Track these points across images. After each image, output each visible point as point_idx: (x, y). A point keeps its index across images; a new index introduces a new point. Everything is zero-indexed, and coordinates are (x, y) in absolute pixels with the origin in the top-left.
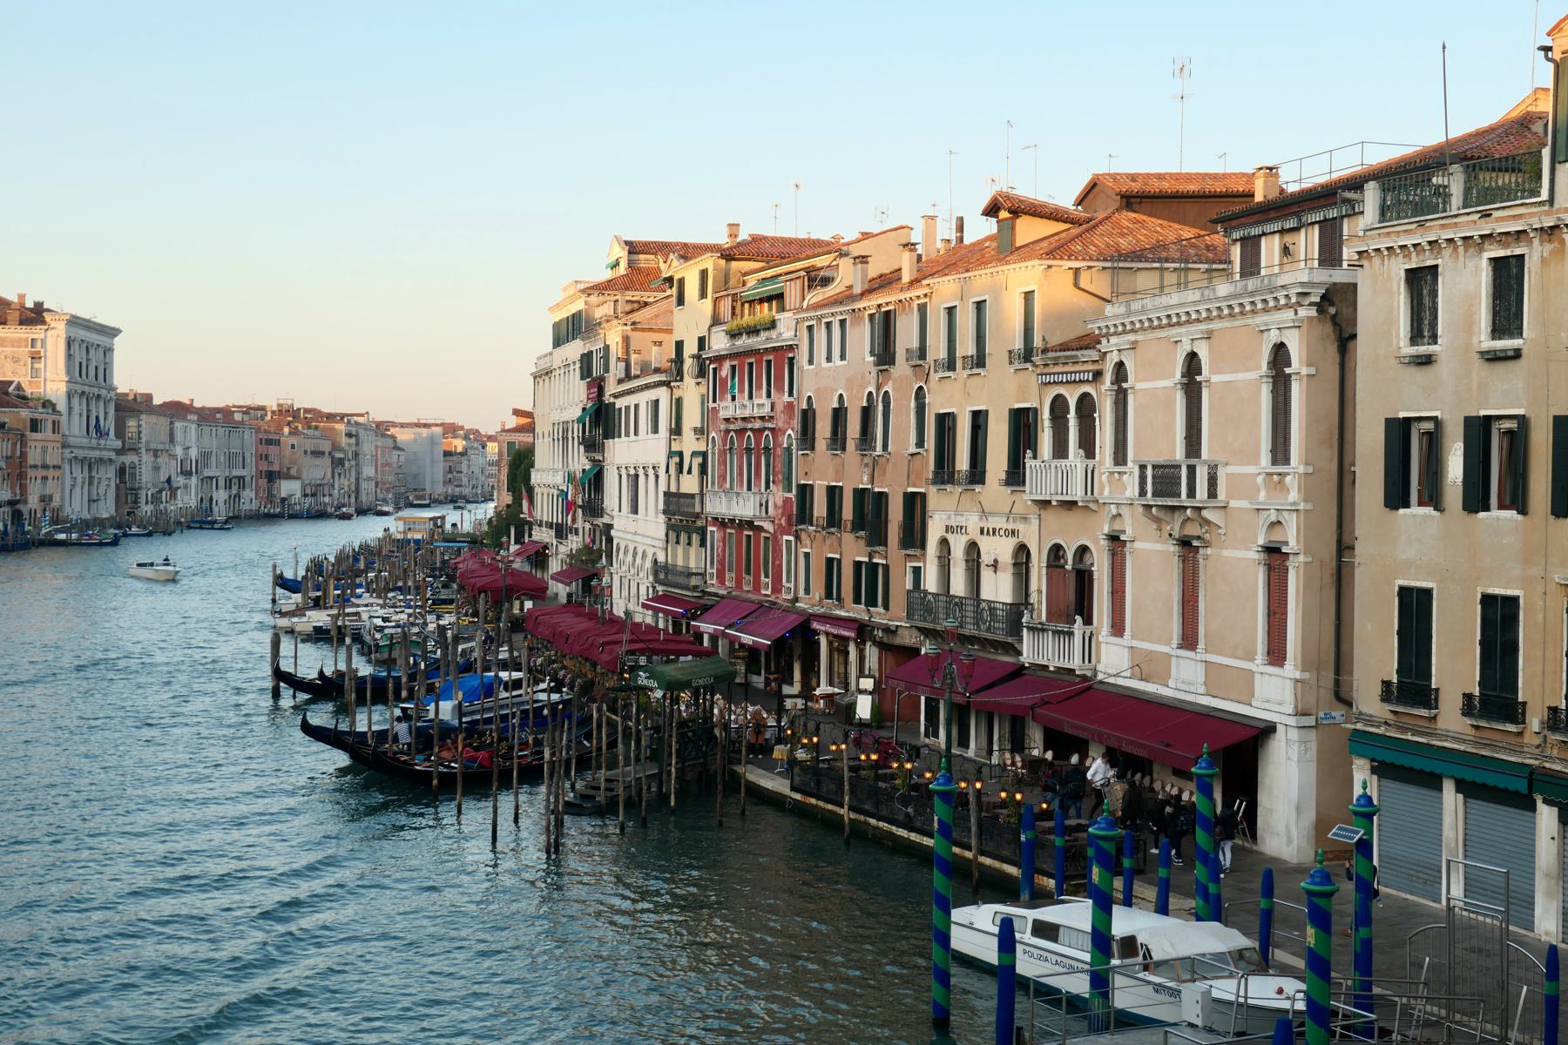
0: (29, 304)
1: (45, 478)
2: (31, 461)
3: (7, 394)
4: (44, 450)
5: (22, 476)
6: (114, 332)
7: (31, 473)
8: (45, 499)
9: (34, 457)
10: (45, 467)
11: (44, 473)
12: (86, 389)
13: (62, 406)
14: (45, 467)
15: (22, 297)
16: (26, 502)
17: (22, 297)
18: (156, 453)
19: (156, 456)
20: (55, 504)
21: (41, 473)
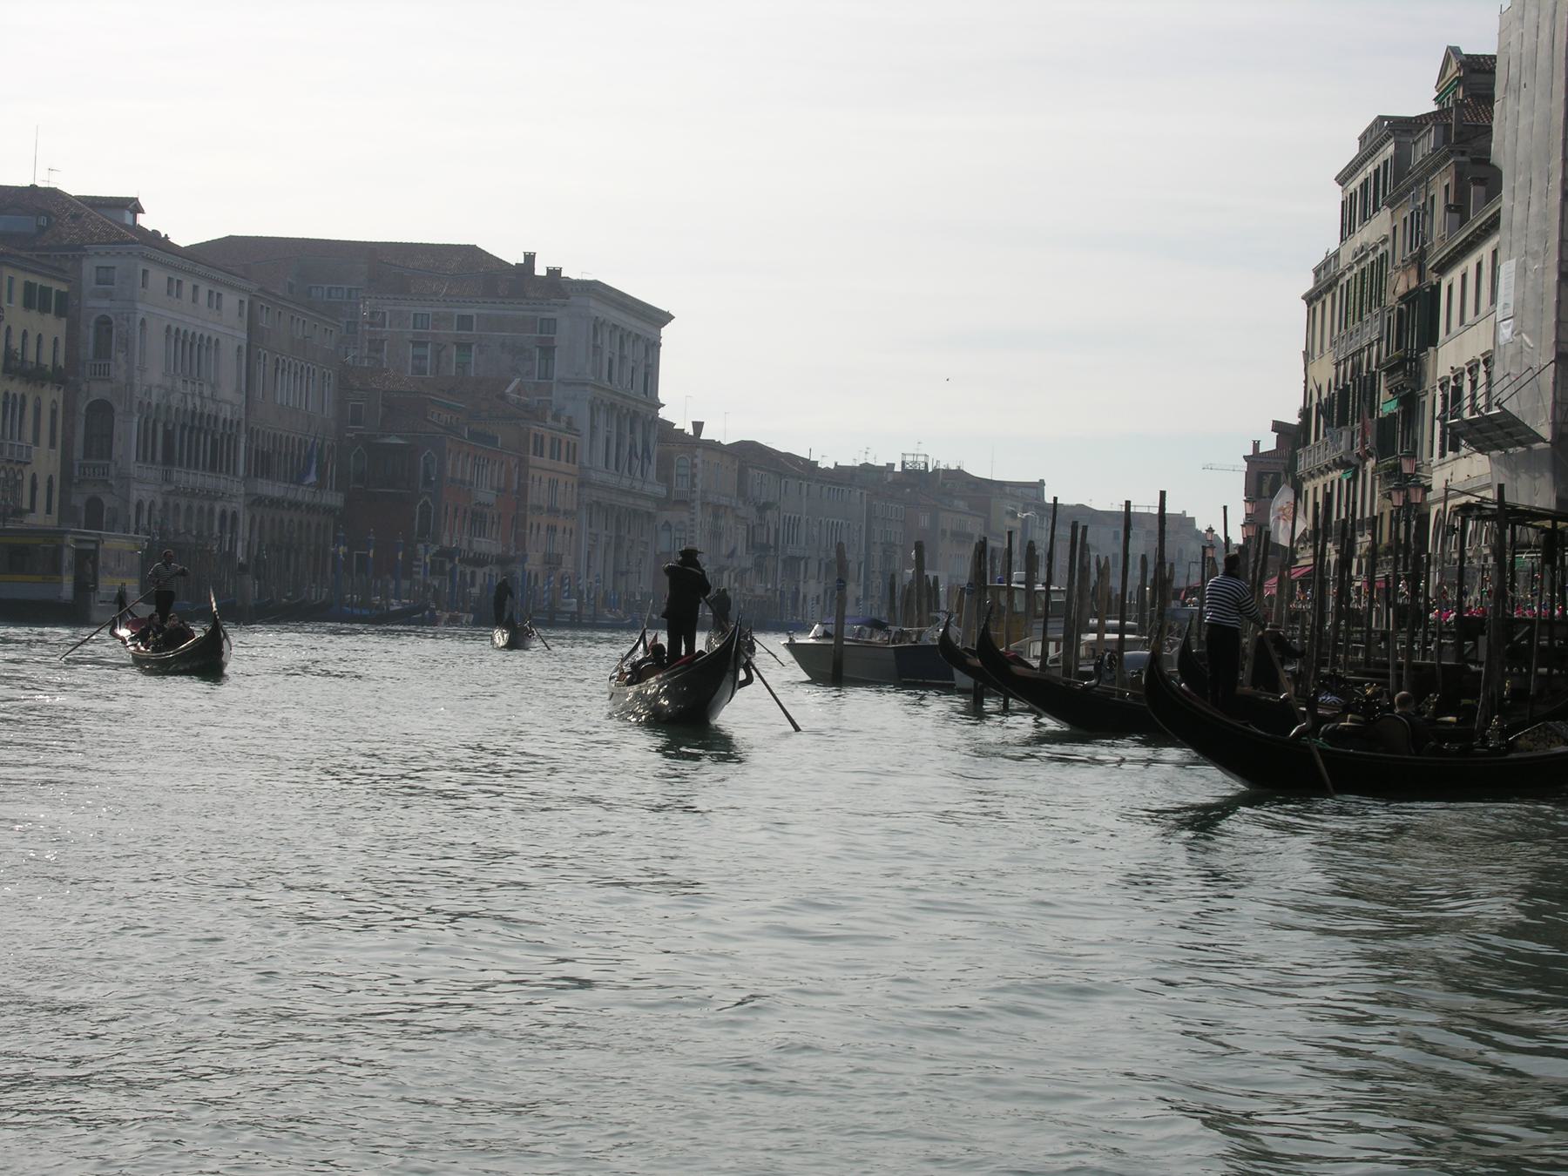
0: (540, 270)
1: (552, 529)
3: (503, 397)
4: (553, 484)
6: (664, 318)
8: (552, 561)
9: (537, 494)
13: (584, 425)
14: (553, 511)
15: (530, 258)
16: (524, 558)
17: (530, 258)
18: (717, 511)
19: (716, 516)
20: (567, 566)
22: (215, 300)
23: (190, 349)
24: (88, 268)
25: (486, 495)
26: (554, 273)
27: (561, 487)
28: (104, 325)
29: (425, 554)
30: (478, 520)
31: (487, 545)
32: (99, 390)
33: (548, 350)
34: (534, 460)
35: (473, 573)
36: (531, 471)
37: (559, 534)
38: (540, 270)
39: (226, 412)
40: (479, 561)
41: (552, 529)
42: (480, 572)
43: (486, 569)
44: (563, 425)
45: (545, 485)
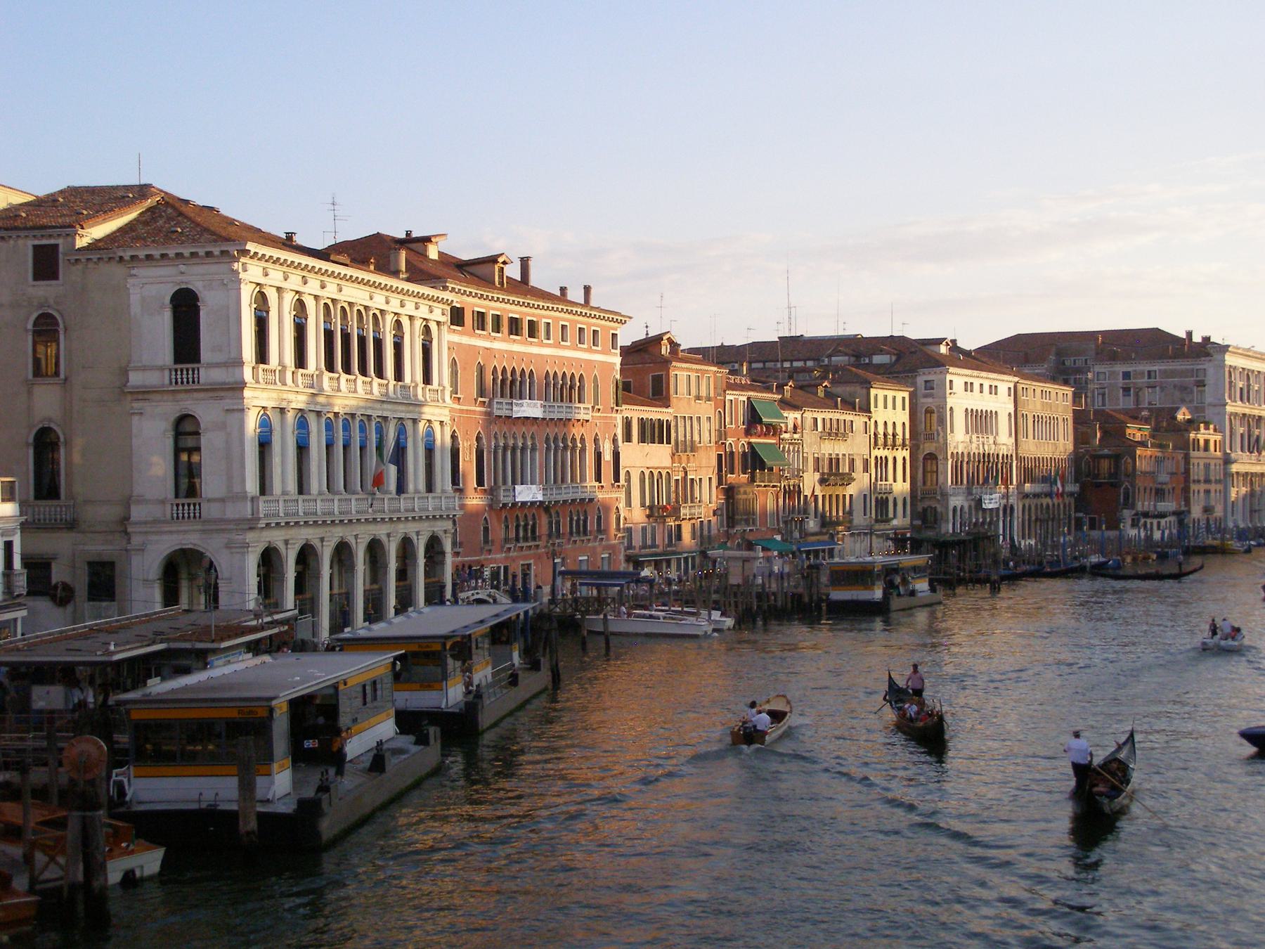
0: (1197, 339)
1: (1207, 492)
2: (1193, 476)
3: (1175, 418)
4: (1207, 466)
5: (1186, 490)
7: (1193, 487)
8: (1207, 510)
9: (1197, 472)
10: (1207, 481)
11: (1207, 486)
12: (1247, 411)
15: (1189, 334)
16: (1189, 512)
17: (1189, 334)
20: (1218, 512)
21: (1202, 487)
22: (994, 390)
23: (981, 421)
24: (920, 380)
25: (1163, 477)
26: (1206, 340)
27: (1212, 467)
28: (929, 412)
29: (1127, 514)
30: (1160, 493)
31: (1168, 505)
32: (928, 448)
33: (1201, 384)
34: (1193, 454)
35: (1159, 523)
36: (1192, 461)
37: (1212, 494)
38: (1197, 339)
39: (1003, 451)
40: (1162, 515)
41: (1207, 492)
42: (1163, 521)
43: (1167, 519)
44: (1211, 431)
45: (1202, 467)
